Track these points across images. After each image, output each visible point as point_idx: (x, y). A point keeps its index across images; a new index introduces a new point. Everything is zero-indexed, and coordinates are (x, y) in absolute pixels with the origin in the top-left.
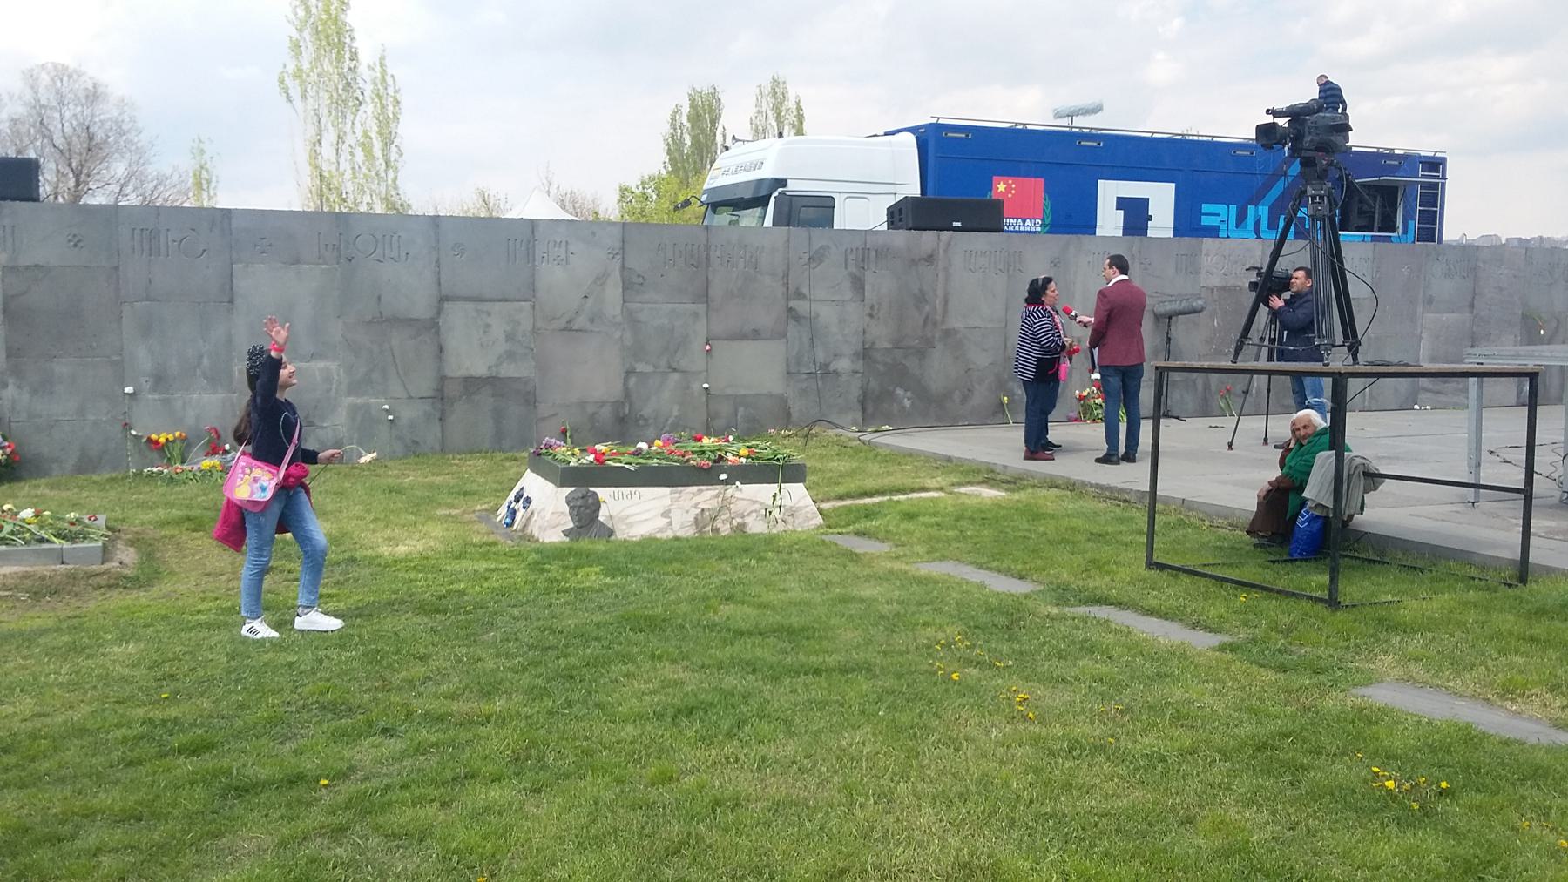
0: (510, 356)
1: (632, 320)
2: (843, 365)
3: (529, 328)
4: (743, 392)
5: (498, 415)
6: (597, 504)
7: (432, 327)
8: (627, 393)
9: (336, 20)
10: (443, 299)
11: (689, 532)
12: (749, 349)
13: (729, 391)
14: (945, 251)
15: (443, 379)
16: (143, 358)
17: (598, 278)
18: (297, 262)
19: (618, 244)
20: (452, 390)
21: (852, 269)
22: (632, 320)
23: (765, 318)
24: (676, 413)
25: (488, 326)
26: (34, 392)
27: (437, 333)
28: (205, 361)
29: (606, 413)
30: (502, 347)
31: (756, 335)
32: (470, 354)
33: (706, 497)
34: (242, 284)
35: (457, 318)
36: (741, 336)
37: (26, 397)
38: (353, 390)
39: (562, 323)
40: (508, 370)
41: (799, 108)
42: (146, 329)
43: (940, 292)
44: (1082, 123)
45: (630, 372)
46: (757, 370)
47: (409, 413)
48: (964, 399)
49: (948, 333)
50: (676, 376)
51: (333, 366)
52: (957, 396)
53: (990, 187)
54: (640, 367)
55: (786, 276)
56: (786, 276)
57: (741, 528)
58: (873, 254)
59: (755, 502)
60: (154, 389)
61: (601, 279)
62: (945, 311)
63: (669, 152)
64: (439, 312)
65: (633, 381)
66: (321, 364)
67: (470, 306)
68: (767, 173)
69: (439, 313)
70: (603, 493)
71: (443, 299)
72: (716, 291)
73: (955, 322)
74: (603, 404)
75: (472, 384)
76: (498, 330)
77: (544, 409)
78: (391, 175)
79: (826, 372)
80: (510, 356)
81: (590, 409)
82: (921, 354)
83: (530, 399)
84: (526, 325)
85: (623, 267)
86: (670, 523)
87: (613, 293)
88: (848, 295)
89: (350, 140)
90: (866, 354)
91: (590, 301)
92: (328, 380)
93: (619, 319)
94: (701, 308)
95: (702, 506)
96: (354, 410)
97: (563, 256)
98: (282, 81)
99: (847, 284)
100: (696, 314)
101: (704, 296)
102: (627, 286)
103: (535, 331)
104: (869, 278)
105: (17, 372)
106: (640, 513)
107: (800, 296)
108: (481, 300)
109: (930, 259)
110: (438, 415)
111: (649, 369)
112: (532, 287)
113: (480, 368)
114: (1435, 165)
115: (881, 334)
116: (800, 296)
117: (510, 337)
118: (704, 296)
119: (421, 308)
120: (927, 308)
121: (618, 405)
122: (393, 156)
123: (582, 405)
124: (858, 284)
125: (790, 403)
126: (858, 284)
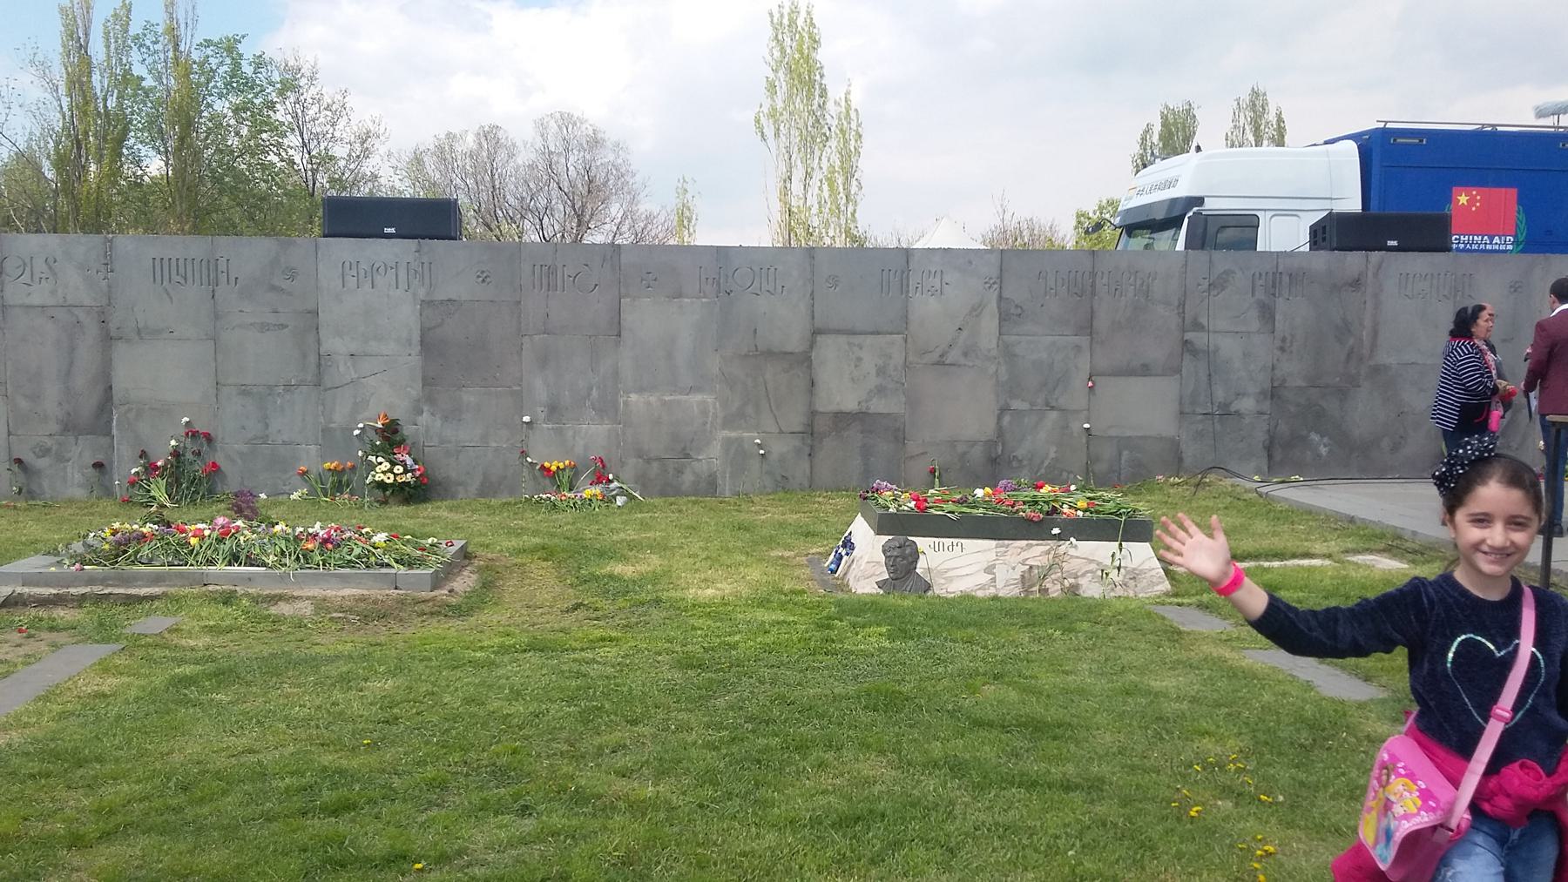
0: (880, 390)
1: (1008, 353)
2: (1247, 405)
3: (901, 361)
4: (1128, 433)
5: (866, 452)
6: (915, 554)
7: (805, 360)
8: (1000, 432)
9: (807, 59)
10: (816, 332)
11: (1015, 591)
12: (1136, 385)
13: (1113, 432)
14: (1376, 275)
15: (813, 414)
16: (539, 388)
17: (974, 309)
18: (680, 296)
19: (995, 273)
20: (821, 425)
21: (1260, 295)
22: (1008, 353)
23: (1156, 352)
24: (1052, 455)
25: (859, 359)
26: (445, 418)
27: (810, 367)
28: (595, 393)
29: (977, 453)
30: (873, 381)
31: (1145, 370)
32: (842, 389)
33: (1035, 552)
34: (628, 318)
35: (829, 351)
36: (1130, 372)
37: (438, 423)
38: (728, 423)
39: (935, 357)
40: (878, 406)
41: (1280, 120)
42: (544, 361)
43: (1368, 323)
45: (1004, 410)
46: (1145, 409)
47: (779, 447)
48: (1395, 448)
49: (1377, 370)
50: (1054, 415)
51: (710, 399)
52: (1386, 443)
53: (1449, 199)
54: (1016, 404)
55: (1182, 305)
56: (1182, 305)
57: (1073, 590)
58: (1286, 279)
59: (1092, 561)
60: (548, 419)
61: (976, 310)
62: (1374, 346)
64: (812, 345)
65: (1007, 419)
66: (699, 397)
67: (842, 339)
69: (811, 347)
70: (922, 543)
71: (816, 332)
72: (1102, 322)
73: (1385, 357)
74: (974, 443)
75: (842, 419)
76: (870, 363)
77: (913, 447)
78: (850, 209)
79: (1226, 413)
80: (880, 390)
81: (961, 448)
82: (1342, 394)
83: (899, 436)
84: (898, 359)
85: (1000, 297)
86: (994, 580)
88: (1255, 325)
89: (817, 175)
90: (1274, 393)
91: (965, 333)
92: (705, 413)
93: (994, 353)
94: (1084, 341)
95: (1030, 562)
96: (728, 443)
97: (938, 286)
98: (758, 121)
99: (1254, 313)
100: (1078, 348)
101: (1088, 327)
102: (1004, 318)
103: (906, 365)
104: (1281, 305)
105: (431, 400)
106: (962, 567)
107: (1197, 326)
108: (853, 333)
109: (1356, 283)
110: (807, 450)
111: (1024, 406)
112: (906, 318)
113: (850, 404)
115: (1294, 370)
116: (1197, 326)
117: (881, 371)
118: (1088, 327)
119: (795, 343)
120: (1351, 341)
121: (991, 444)
122: (854, 189)
123: (953, 443)
124: (1267, 314)
125: (1183, 447)
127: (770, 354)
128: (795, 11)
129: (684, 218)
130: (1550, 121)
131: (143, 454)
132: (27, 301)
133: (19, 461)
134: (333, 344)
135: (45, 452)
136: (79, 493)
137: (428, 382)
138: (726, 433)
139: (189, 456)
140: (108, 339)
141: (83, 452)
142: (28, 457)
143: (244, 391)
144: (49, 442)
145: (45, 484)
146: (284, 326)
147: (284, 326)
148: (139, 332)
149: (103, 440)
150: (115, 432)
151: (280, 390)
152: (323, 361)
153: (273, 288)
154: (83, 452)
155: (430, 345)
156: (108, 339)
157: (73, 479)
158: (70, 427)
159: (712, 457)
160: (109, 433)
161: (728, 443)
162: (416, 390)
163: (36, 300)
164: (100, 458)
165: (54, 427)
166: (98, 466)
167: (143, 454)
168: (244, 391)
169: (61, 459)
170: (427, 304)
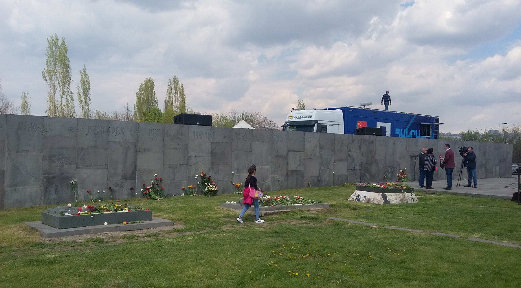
2: (357, 168)
6: (386, 197)
7: (286, 158)
9: (64, 56)
10: (289, 151)
11: (400, 203)
15: (288, 170)
22: (321, 156)
28: (246, 166)
29: (316, 179)
31: (342, 160)
33: (400, 195)
40: (299, 169)
41: (182, 87)
44: (367, 107)
45: (320, 169)
46: (341, 169)
48: (378, 176)
49: (376, 160)
51: (269, 167)
53: (357, 123)
54: (323, 168)
57: (407, 202)
60: (237, 173)
63: (139, 99)
66: (266, 167)
67: (293, 152)
68: (313, 119)
73: (377, 158)
74: (315, 177)
75: (293, 171)
78: (87, 107)
79: (355, 170)
80: (299, 165)
87: (318, 150)
88: (358, 150)
89: (66, 94)
90: (361, 165)
94: (333, 153)
98: (44, 74)
101: (333, 151)
103: (304, 159)
104: (362, 146)
106: (393, 198)
107: (350, 151)
113: (294, 169)
114: (437, 120)
116: (350, 151)
117: (300, 160)
118: (333, 151)
119: (284, 154)
121: (318, 177)
122: (88, 100)
124: (360, 148)
126: (360, 148)
127: (280, 156)
128: (57, 38)
129: (25, 105)
130: (362, 107)
131: (144, 185)
132: (115, 140)
133: (110, 188)
134: (192, 154)
135: (118, 185)
136: (126, 197)
137: (212, 163)
138: (271, 176)
139: (155, 185)
140: (136, 152)
141: (128, 185)
142: (113, 187)
143: (170, 167)
144: (118, 182)
145: (117, 195)
146: (180, 149)
147: (180, 149)
148: (144, 150)
149: (133, 181)
150: (136, 179)
151: (178, 166)
152: (189, 158)
153: (178, 138)
154: (128, 185)
155: (213, 154)
156: (136, 152)
157: (124, 193)
158: (125, 178)
159: (269, 182)
160: (135, 179)
161: (272, 177)
162: (209, 166)
163: (117, 140)
164: (132, 186)
165: (120, 178)
166: (132, 189)
167: (144, 185)
168: (170, 167)
169: (122, 187)
170: (212, 143)
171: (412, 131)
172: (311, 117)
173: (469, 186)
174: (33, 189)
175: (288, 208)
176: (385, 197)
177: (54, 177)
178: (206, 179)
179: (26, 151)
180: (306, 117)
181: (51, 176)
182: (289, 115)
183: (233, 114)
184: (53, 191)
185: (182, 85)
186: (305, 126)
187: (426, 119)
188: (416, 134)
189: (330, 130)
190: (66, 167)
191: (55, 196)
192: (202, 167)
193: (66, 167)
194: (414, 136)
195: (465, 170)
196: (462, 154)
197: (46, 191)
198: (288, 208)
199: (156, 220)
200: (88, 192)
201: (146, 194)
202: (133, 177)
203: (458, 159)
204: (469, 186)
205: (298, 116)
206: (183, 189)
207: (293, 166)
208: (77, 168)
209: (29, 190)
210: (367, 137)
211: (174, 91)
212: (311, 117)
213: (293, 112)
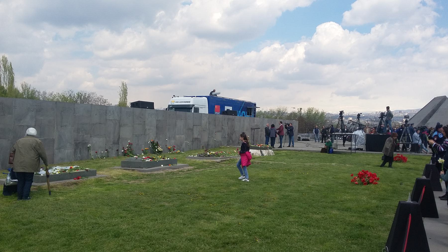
7: (192, 130)
31: (219, 131)
33: (267, 151)
46: (218, 137)
53: (215, 107)
90: (228, 135)
101: (215, 126)
106: (265, 152)
113: (196, 137)
114: (255, 105)
118: (215, 126)
131: (123, 148)
134: (147, 127)
135: (110, 148)
136: (114, 156)
137: (157, 134)
140: (120, 126)
141: (115, 148)
143: (136, 136)
144: (111, 146)
152: (145, 130)
156: (120, 126)
158: (114, 143)
161: (186, 143)
162: (155, 135)
163: (111, 119)
165: (112, 143)
166: (117, 150)
167: (123, 148)
169: (112, 149)
170: (157, 120)
171: (243, 112)
172: (189, 102)
173: (289, 146)
174: (68, 151)
175: (228, 158)
176: (261, 152)
177: (79, 143)
178: (154, 145)
179: (66, 126)
180: (186, 102)
181: (78, 142)
182: (171, 100)
183: (70, 92)
184: (79, 152)
185: (11, 64)
186: (186, 108)
187: (250, 104)
188: (244, 114)
189: (201, 111)
190: (85, 136)
191: (79, 155)
192: (151, 137)
193: (85, 136)
194: (244, 116)
195: (288, 137)
196: (286, 128)
197: (75, 152)
198: (228, 158)
199: (179, 164)
200: (96, 152)
201: (125, 154)
202: (118, 143)
203: (285, 131)
204: (289, 146)
205: (180, 101)
206: (143, 150)
207: (196, 136)
208: (91, 137)
209: (66, 151)
210: (231, 116)
211: (3, 70)
212: (189, 102)
213: (174, 98)
